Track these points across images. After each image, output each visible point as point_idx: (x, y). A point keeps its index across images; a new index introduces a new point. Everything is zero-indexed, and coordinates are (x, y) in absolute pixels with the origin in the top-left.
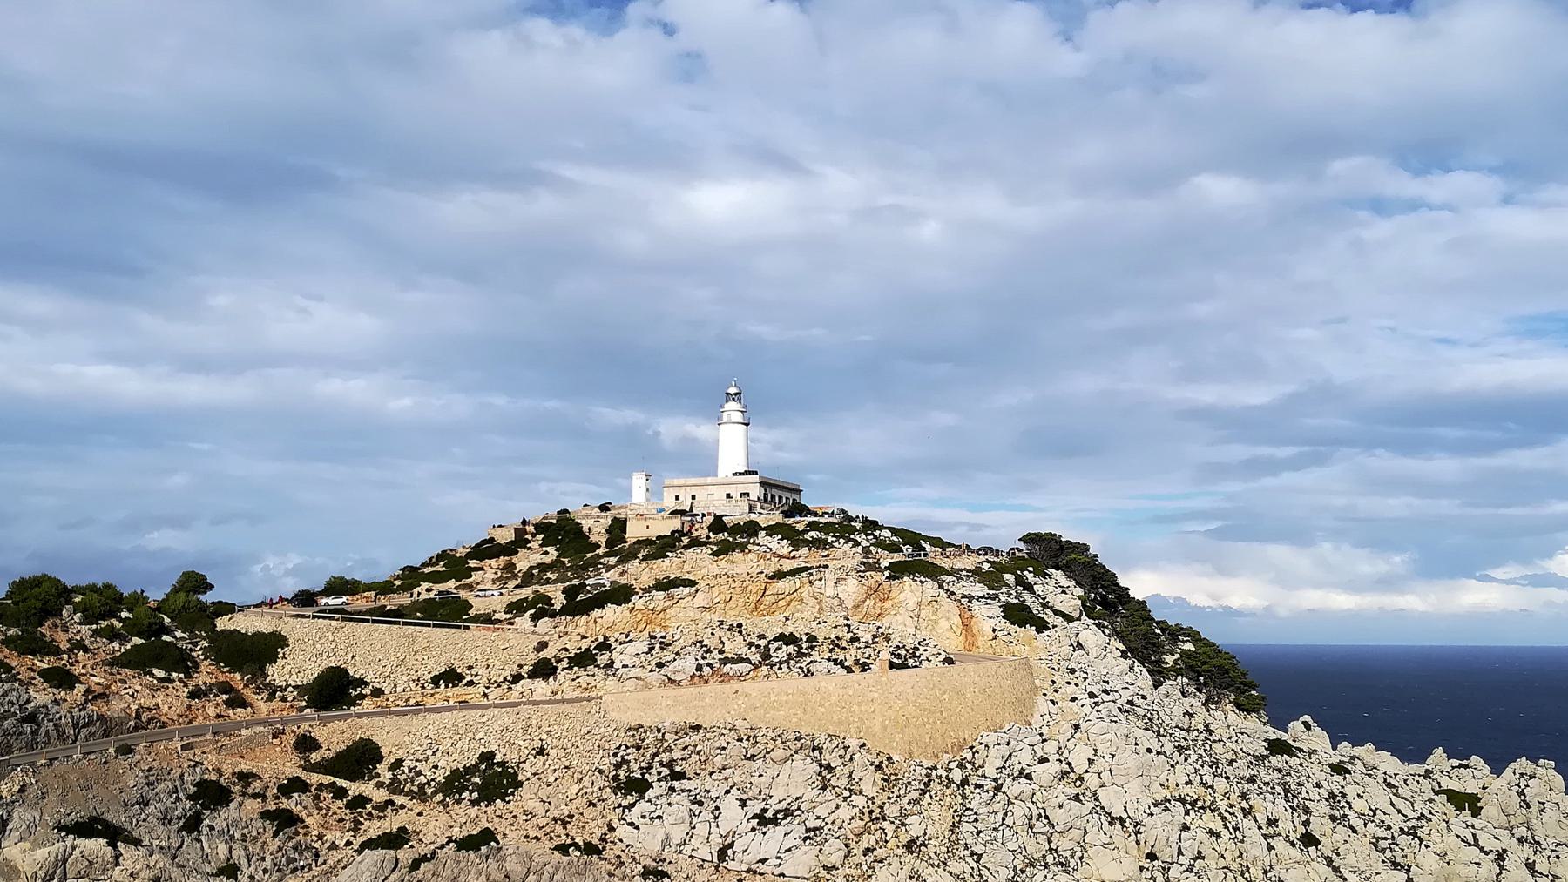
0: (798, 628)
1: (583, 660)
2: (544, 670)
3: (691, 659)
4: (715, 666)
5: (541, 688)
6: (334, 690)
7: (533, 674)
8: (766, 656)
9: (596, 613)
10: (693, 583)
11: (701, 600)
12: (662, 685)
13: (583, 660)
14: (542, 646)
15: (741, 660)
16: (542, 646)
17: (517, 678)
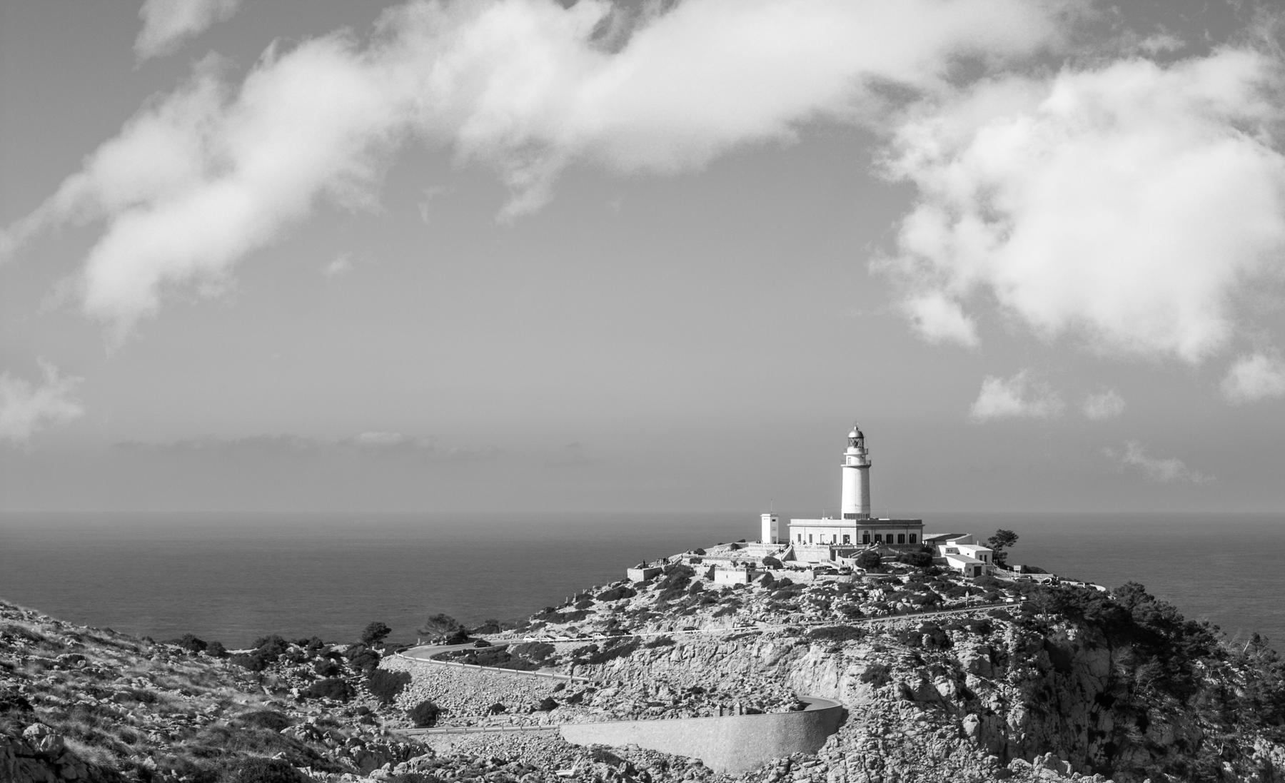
0: (706, 684)
1: (575, 700)
2: (549, 705)
3: (632, 702)
4: (646, 708)
5: (543, 717)
6: (428, 715)
7: (542, 709)
8: (676, 702)
9: (610, 663)
10: (673, 643)
11: (674, 656)
12: (610, 718)
13: (575, 700)
14: (561, 687)
15: (659, 704)
16: (561, 687)
17: (533, 710)
